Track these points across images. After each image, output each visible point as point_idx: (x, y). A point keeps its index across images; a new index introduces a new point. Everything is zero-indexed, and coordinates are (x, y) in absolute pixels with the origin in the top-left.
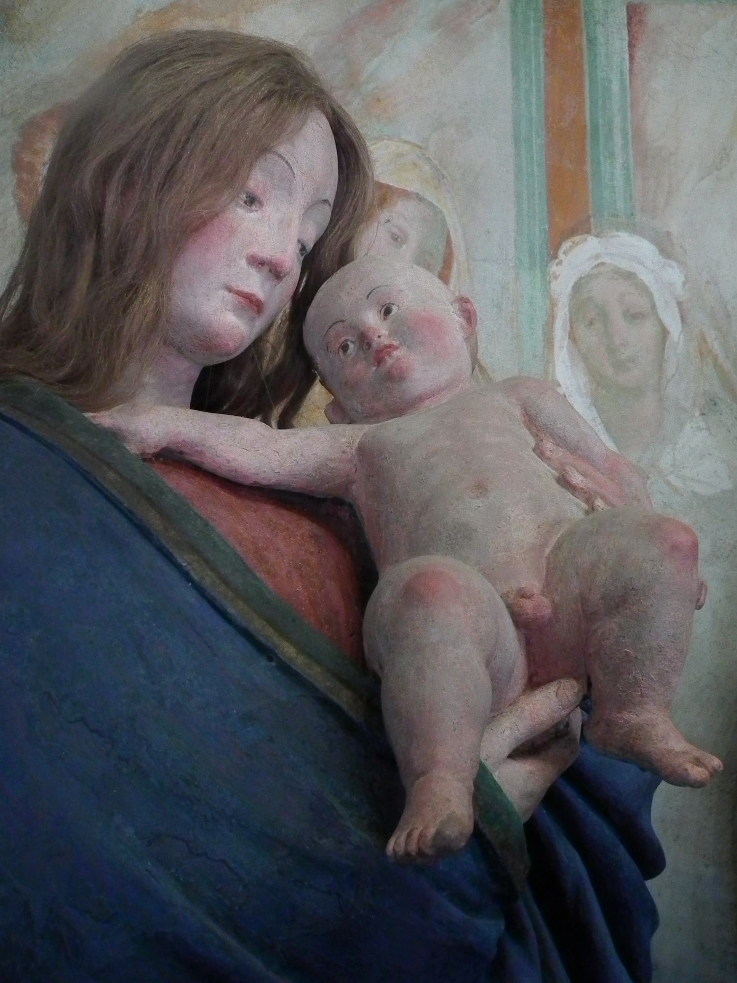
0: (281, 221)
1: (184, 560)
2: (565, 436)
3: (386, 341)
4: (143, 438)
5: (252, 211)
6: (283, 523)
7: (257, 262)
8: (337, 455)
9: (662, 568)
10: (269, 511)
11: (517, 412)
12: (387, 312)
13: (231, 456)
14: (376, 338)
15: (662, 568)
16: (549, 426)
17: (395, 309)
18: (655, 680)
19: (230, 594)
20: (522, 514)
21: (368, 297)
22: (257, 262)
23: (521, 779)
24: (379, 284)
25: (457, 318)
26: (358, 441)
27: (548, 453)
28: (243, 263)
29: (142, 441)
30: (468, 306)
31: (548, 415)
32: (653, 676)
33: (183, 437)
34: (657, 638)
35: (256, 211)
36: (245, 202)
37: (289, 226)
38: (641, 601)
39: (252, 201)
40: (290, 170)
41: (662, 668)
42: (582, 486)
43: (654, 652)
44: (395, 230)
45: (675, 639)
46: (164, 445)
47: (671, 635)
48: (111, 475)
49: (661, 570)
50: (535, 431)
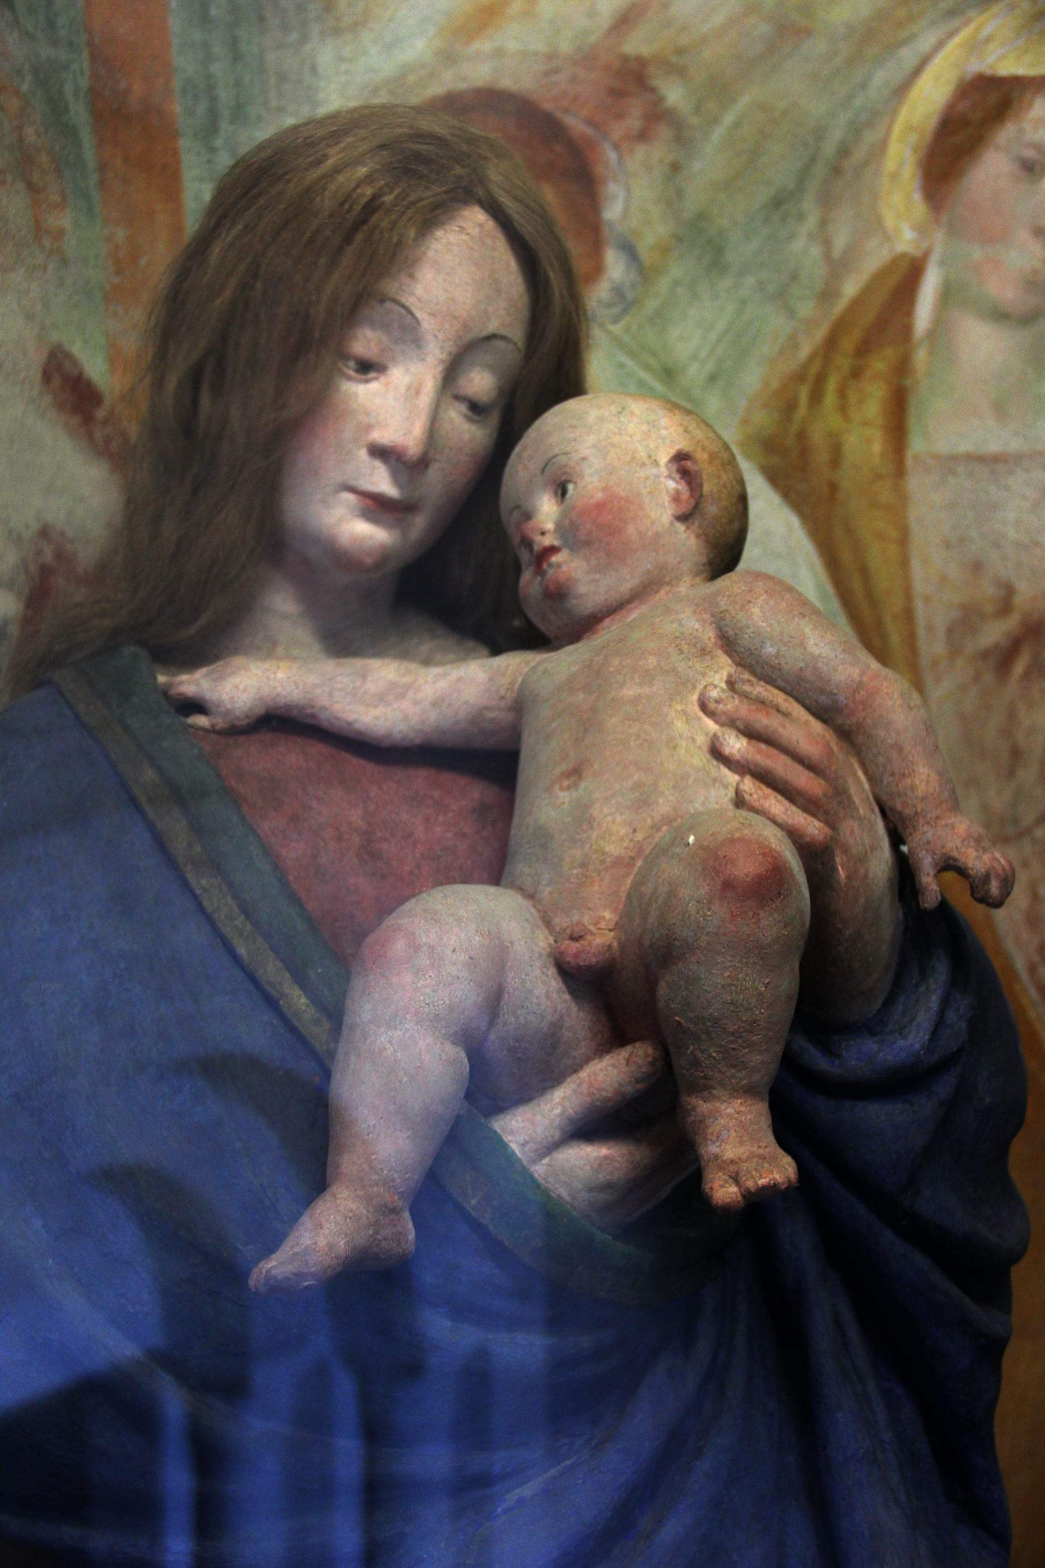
0: (409, 388)
1: (202, 882)
2: (779, 664)
3: (548, 541)
4: (227, 710)
5: (367, 381)
6: (436, 794)
7: (381, 452)
8: (494, 703)
9: (709, 913)
10: (420, 778)
11: (709, 635)
12: (563, 492)
13: (351, 717)
14: (538, 538)
15: (709, 913)
16: (754, 651)
17: (570, 487)
18: (718, 1058)
19: (249, 927)
20: (611, 814)
21: (543, 471)
22: (381, 452)
23: (588, 1167)
24: (557, 451)
25: (672, 485)
26: (520, 680)
27: (712, 706)
28: (363, 454)
29: (228, 712)
30: (688, 464)
31: (752, 635)
32: (714, 1054)
33: (283, 701)
34: (709, 1005)
35: (376, 379)
36: (357, 371)
37: (418, 392)
38: (686, 955)
39: (367, 368)
40: (409, 316)
41: (723, 1043)
42: (737, 756)
43: (709, 1024)
44: (1030, 154)
45: (737, 1008)
46: (262, 712)
47: (729, 1002)
48: (149, 774)
49: (708, 916)
50: (737, 659)
